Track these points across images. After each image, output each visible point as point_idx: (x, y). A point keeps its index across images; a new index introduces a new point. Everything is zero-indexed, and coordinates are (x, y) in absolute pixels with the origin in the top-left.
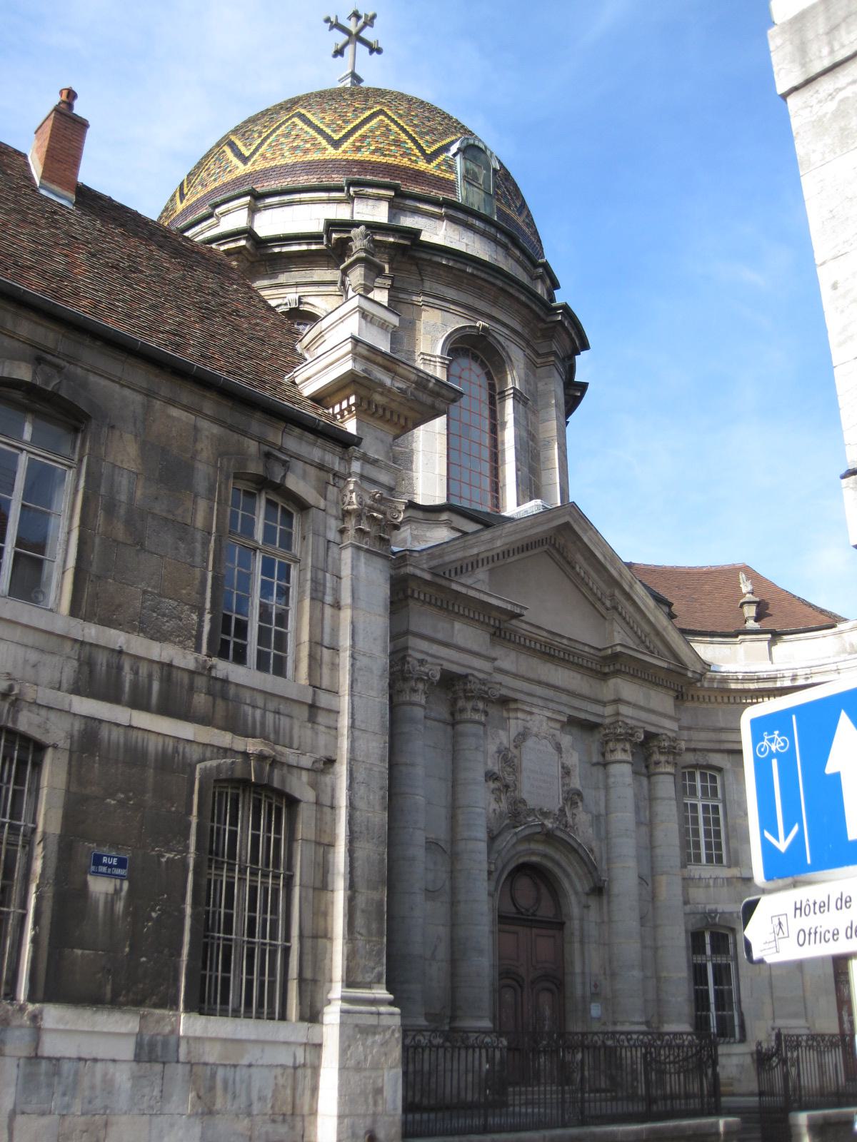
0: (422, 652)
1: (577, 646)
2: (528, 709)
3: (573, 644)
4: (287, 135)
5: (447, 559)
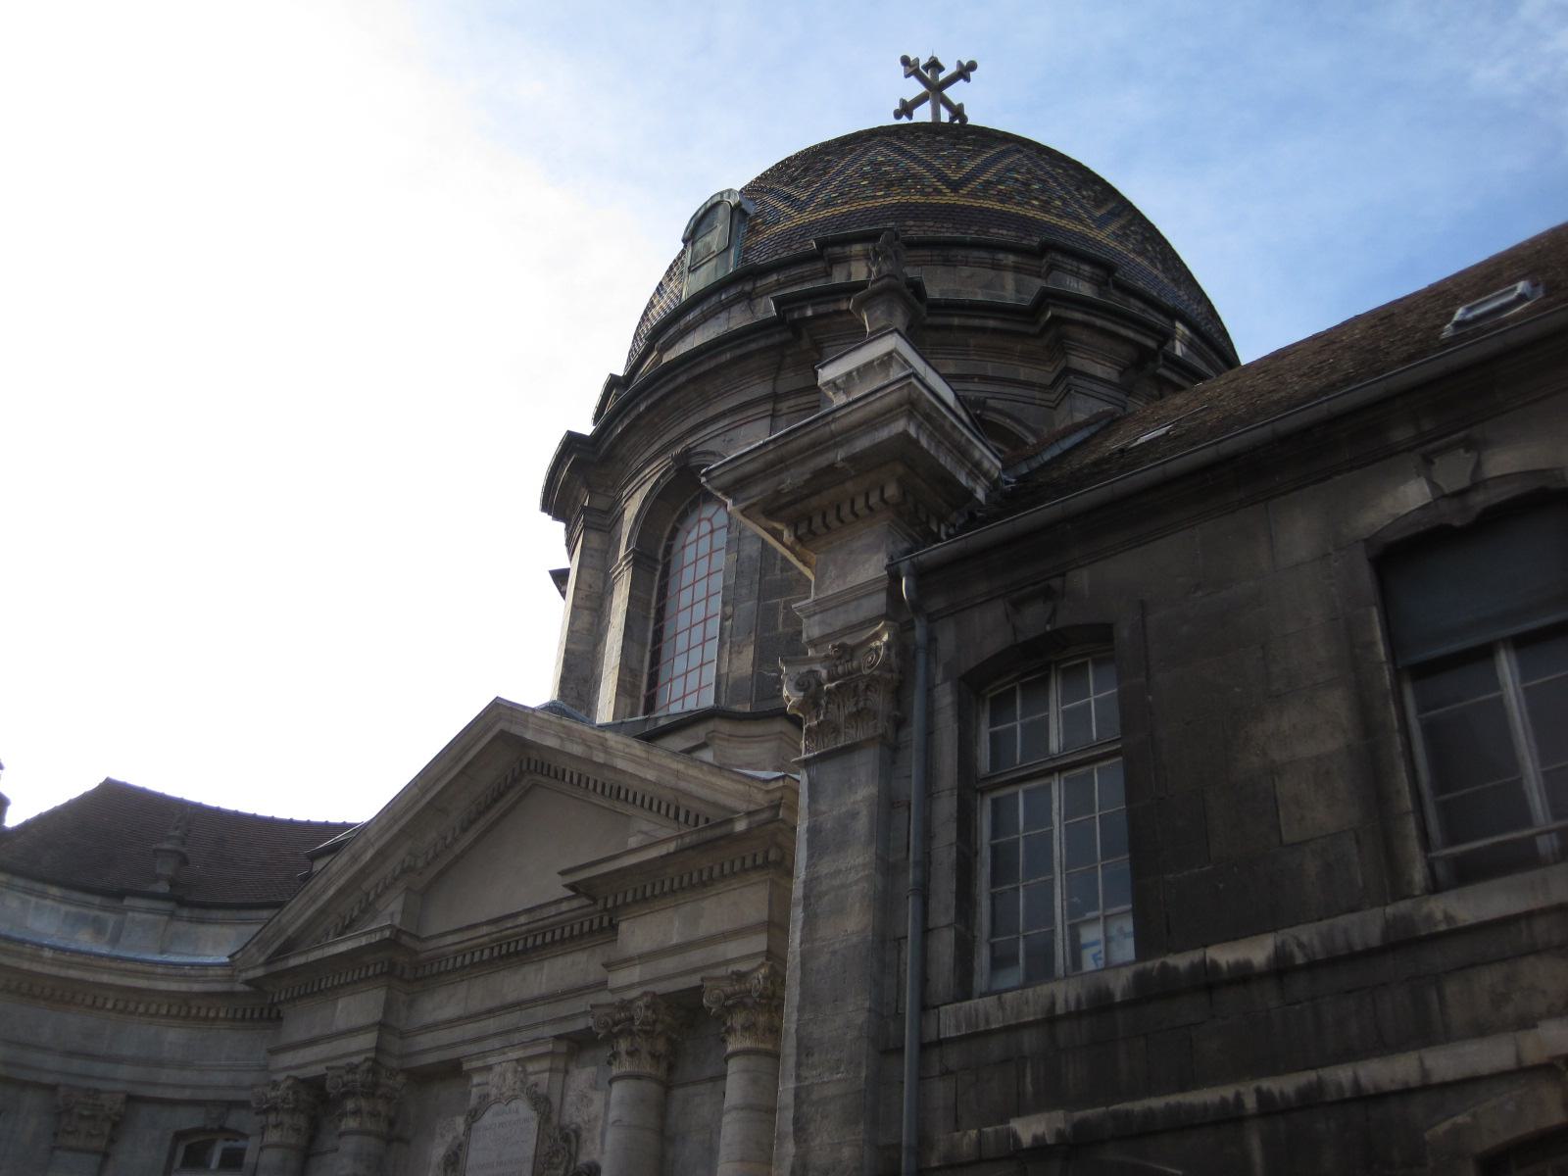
0: (286, 1069)
1: (545, 913)
2: (480, 1064)
3: (538, 915)
5: (290, 931)
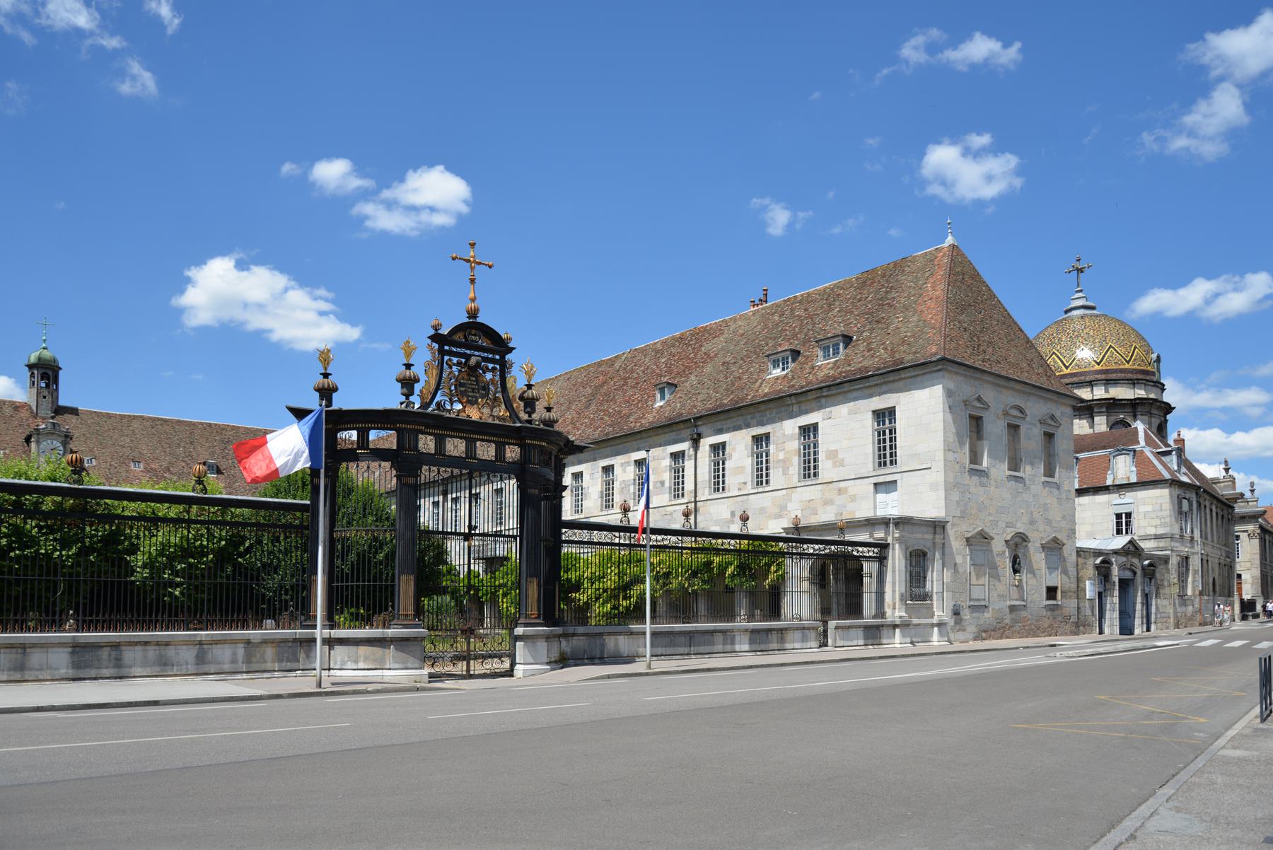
4: (1112, 357)
